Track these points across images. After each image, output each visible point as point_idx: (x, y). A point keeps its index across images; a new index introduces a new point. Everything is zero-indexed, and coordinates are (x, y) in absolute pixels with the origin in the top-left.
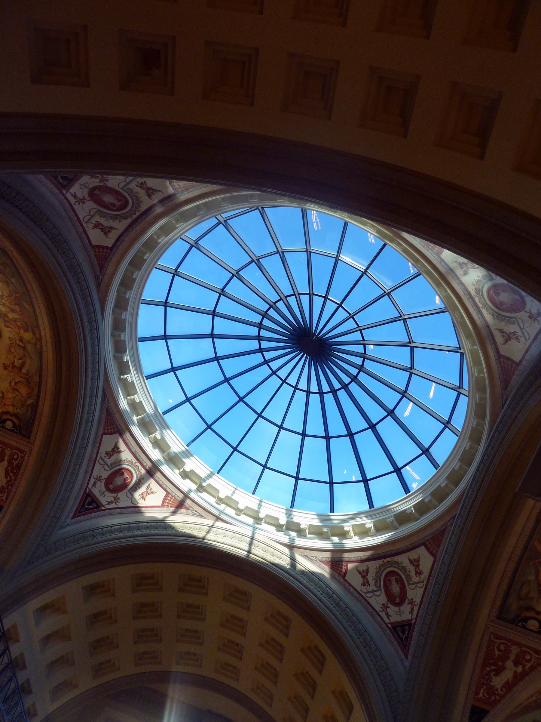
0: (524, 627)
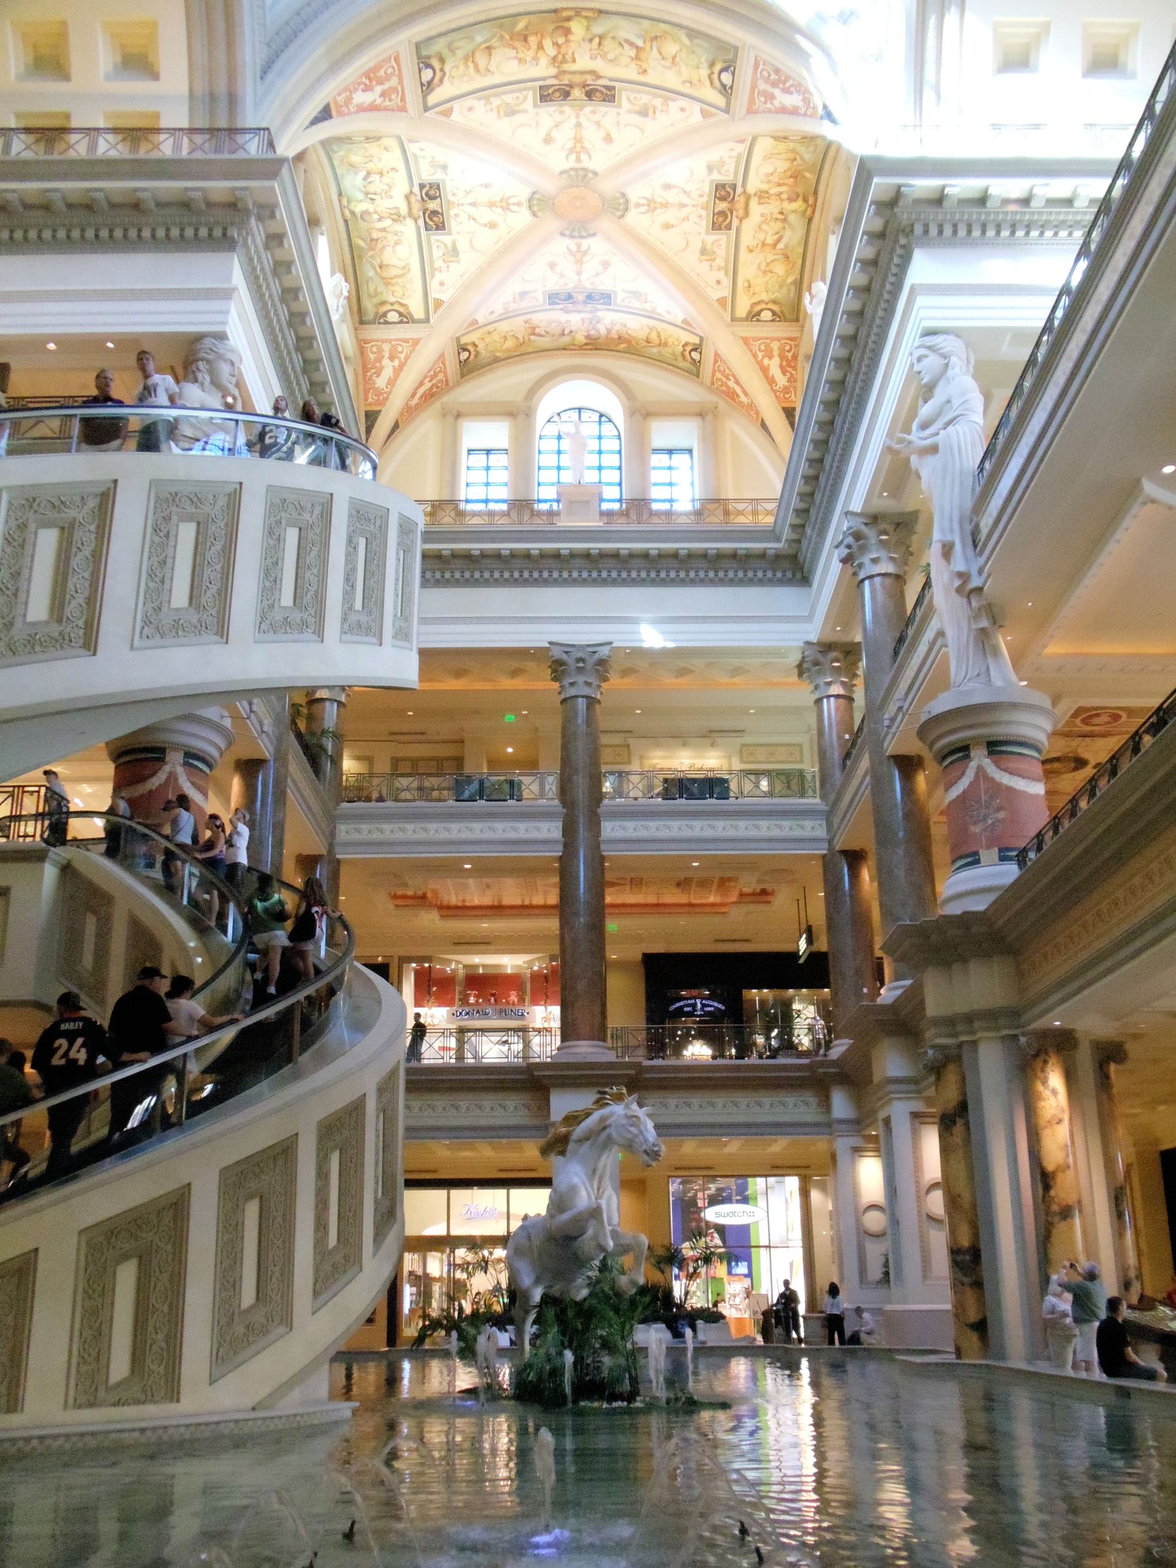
0: (387, 323)
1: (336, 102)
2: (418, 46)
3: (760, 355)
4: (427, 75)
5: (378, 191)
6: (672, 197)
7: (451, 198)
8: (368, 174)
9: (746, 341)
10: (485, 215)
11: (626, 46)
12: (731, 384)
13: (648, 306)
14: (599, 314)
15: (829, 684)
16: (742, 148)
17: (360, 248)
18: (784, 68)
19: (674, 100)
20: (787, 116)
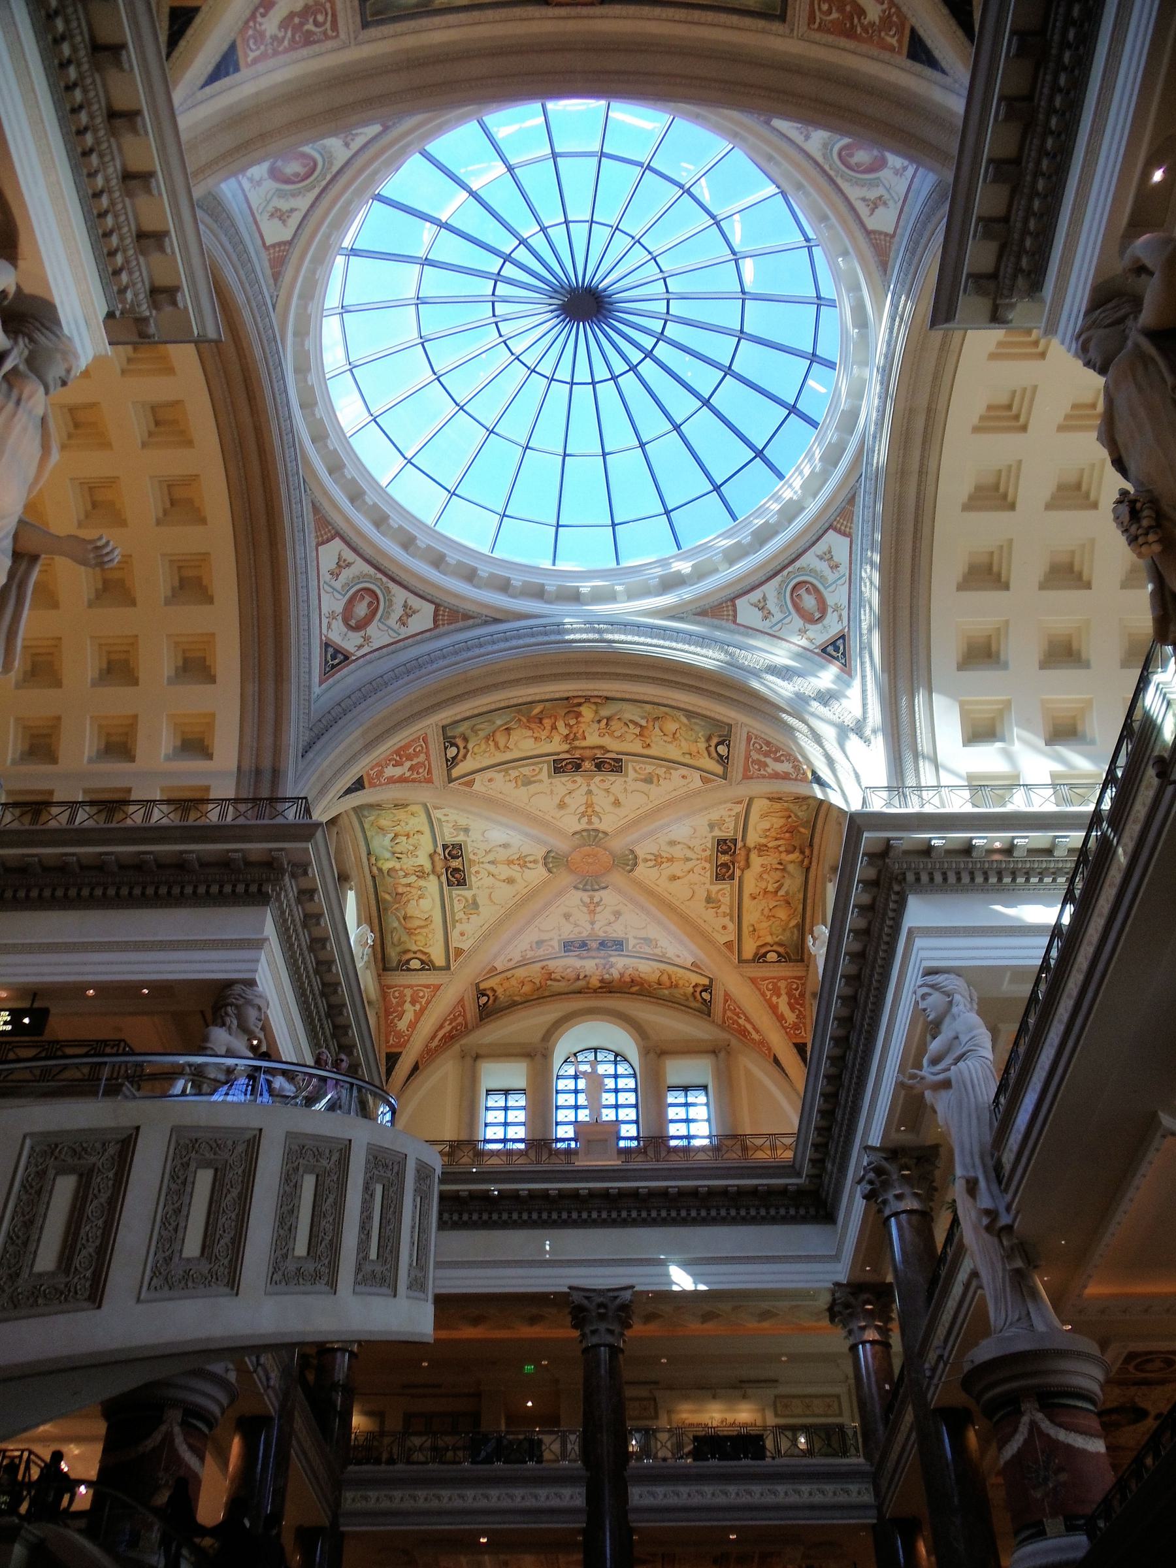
1: (368, 775)
2: (444, 728)
3: (768, 993)
4: (452, 752)
5: (405, 850)
6: (677, 852)
7: (471, 856)
8: (396, 836)
9: (753, 981)
10: (505, 871)
11: (631, 726)
12: (741, 1021)
13: (658, 951)
14: (613, 959)
15: (863, 1329)
16: (739, 808)
17: (385, 900)
18: (774, 742)
19: (676, 769)
20: (780, 781)
